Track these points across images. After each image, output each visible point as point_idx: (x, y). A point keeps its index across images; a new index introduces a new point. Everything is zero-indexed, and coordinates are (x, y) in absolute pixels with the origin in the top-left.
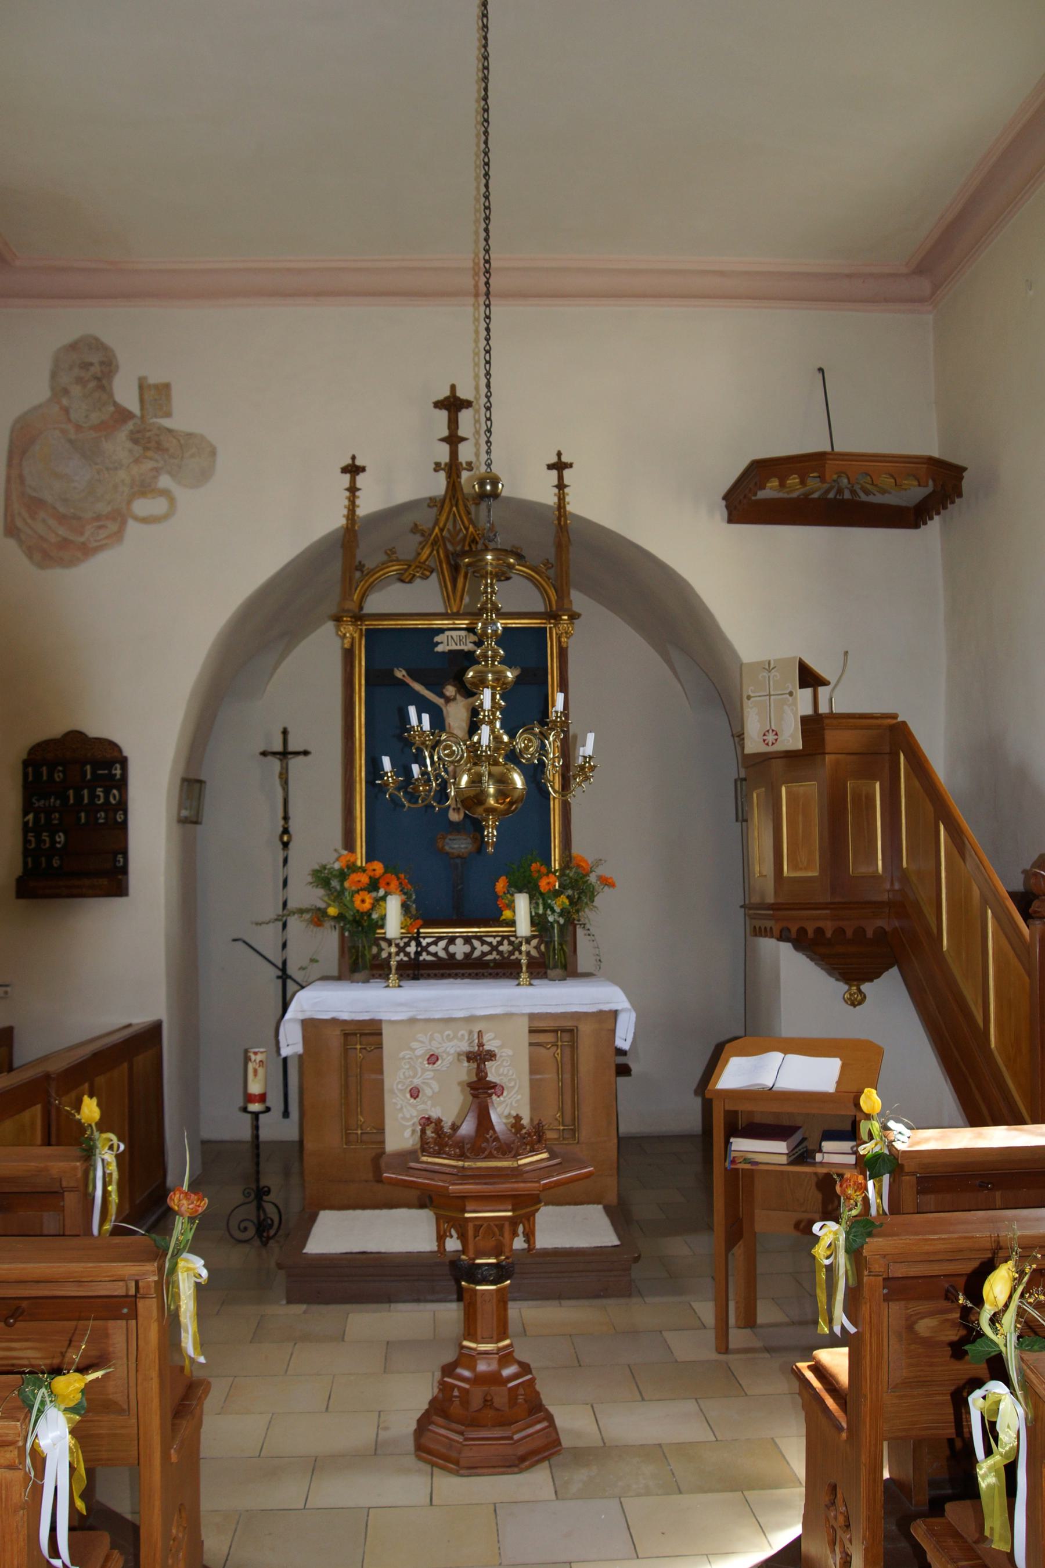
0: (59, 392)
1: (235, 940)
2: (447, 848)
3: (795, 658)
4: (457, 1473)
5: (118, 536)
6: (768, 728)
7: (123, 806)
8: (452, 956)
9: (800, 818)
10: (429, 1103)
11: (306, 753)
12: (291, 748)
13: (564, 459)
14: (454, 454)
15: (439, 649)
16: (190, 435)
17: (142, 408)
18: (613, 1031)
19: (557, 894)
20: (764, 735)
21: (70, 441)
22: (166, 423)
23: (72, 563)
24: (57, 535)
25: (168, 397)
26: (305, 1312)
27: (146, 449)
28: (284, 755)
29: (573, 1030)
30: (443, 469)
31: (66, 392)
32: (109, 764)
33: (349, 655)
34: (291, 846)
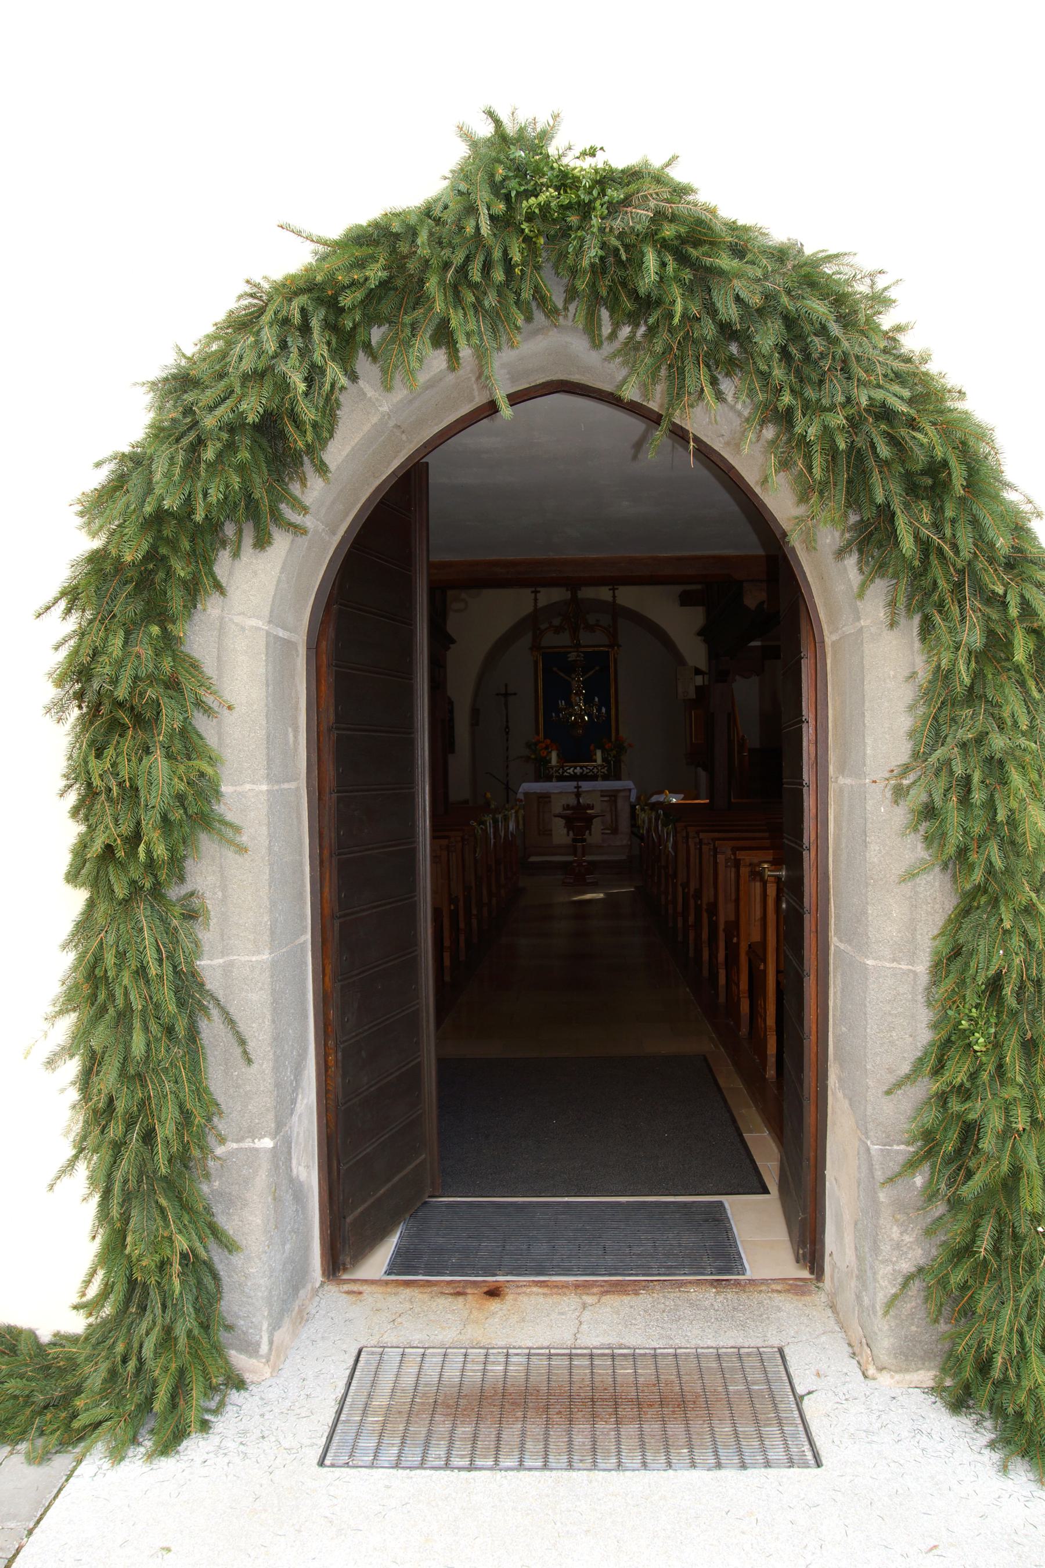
8: (575, 773)
11: (515, 694)
28: (506, 695)
33: (536, 663)
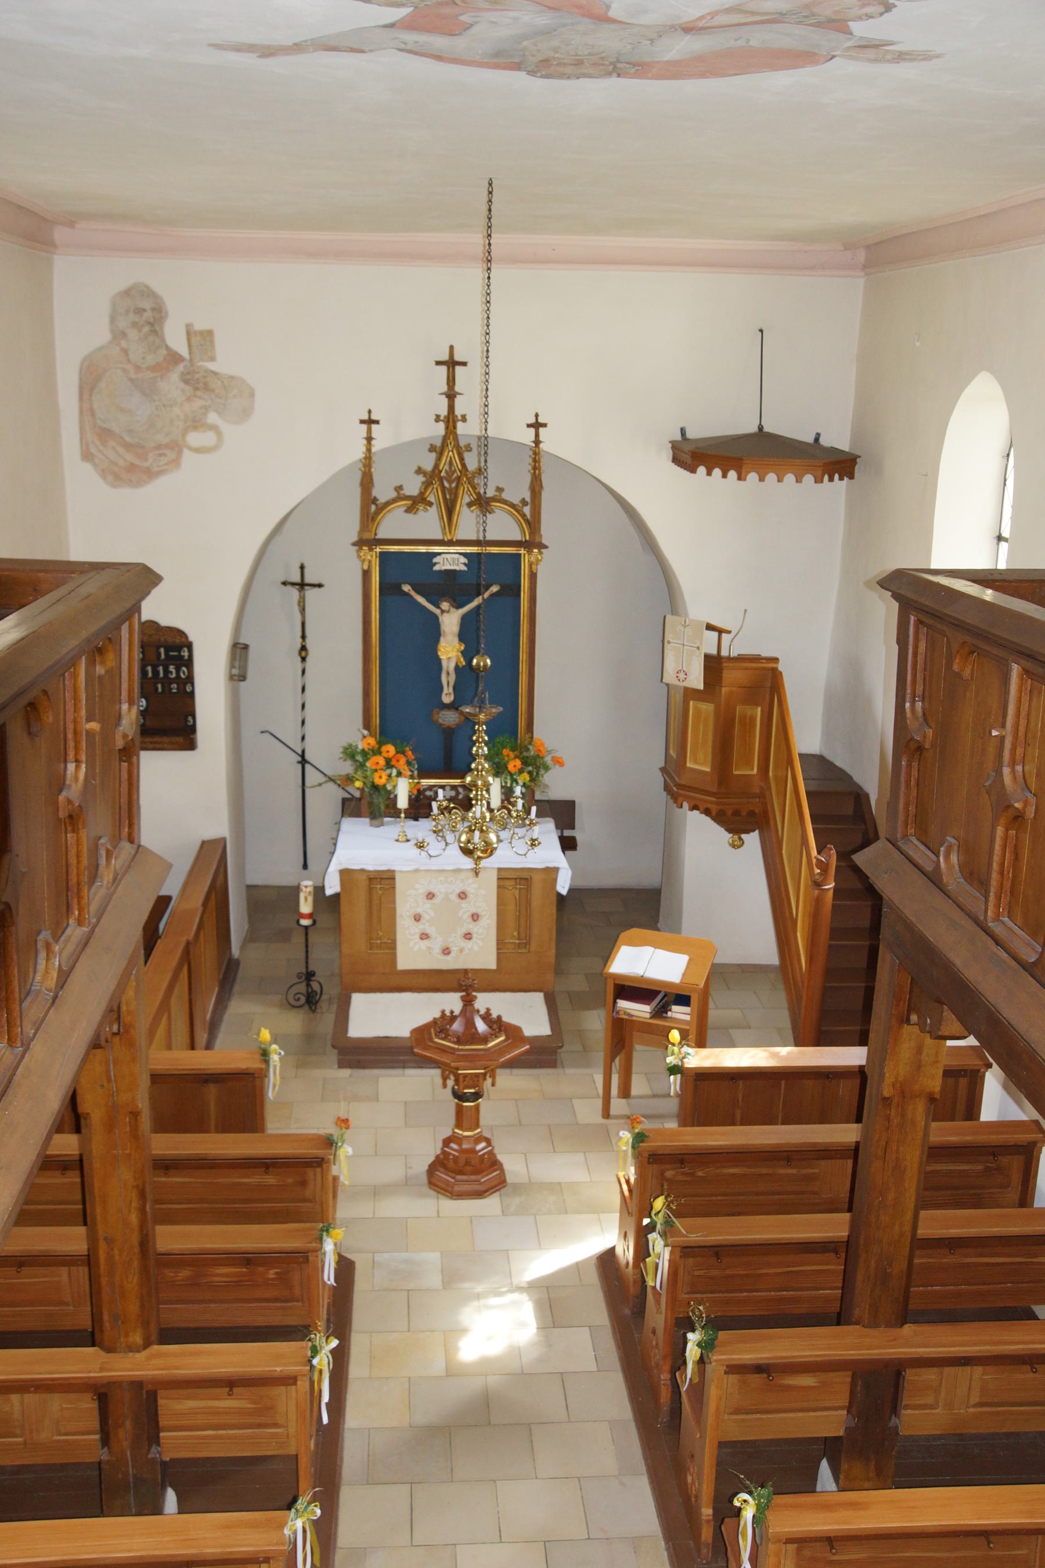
0: (119, 335)
1: (262, 732)
2: (440, 721)
3: (704, 622)
4: (451, 1198)
5: (176, 462)
6: (681, 669)
7: (190, 679)
9: (701, 727)
10: (428, 924)
11: (320, 586)
12: (307, 580)
13: (540, 420)
14: (451, 408)
15: (436, 568)
16: (232, 378)
17: (190, 353)
18: (555, 880)
19: (521, 771)
20: (678, 673)
21: (131, 380)
22: (211, 366)
23: (138, 484)
24: (125, 460)
25: (212, 342)
26: (351, 1076)
27: (197, 389)
29: (527, 879)
30: (443, 421)
31: (124, 334)
32: (179, 648)
33: (366, 574)
34: (308, 659)
